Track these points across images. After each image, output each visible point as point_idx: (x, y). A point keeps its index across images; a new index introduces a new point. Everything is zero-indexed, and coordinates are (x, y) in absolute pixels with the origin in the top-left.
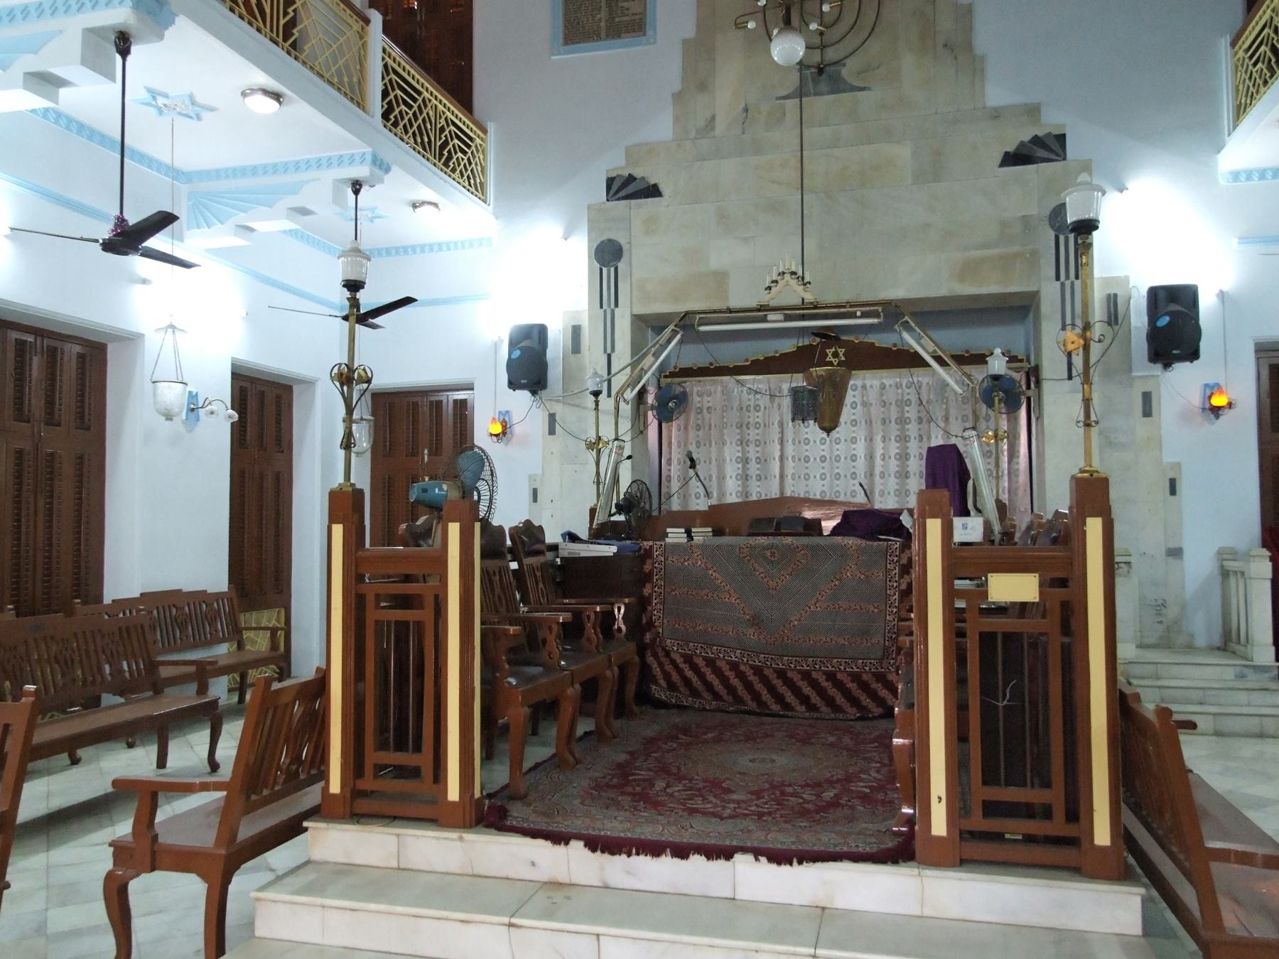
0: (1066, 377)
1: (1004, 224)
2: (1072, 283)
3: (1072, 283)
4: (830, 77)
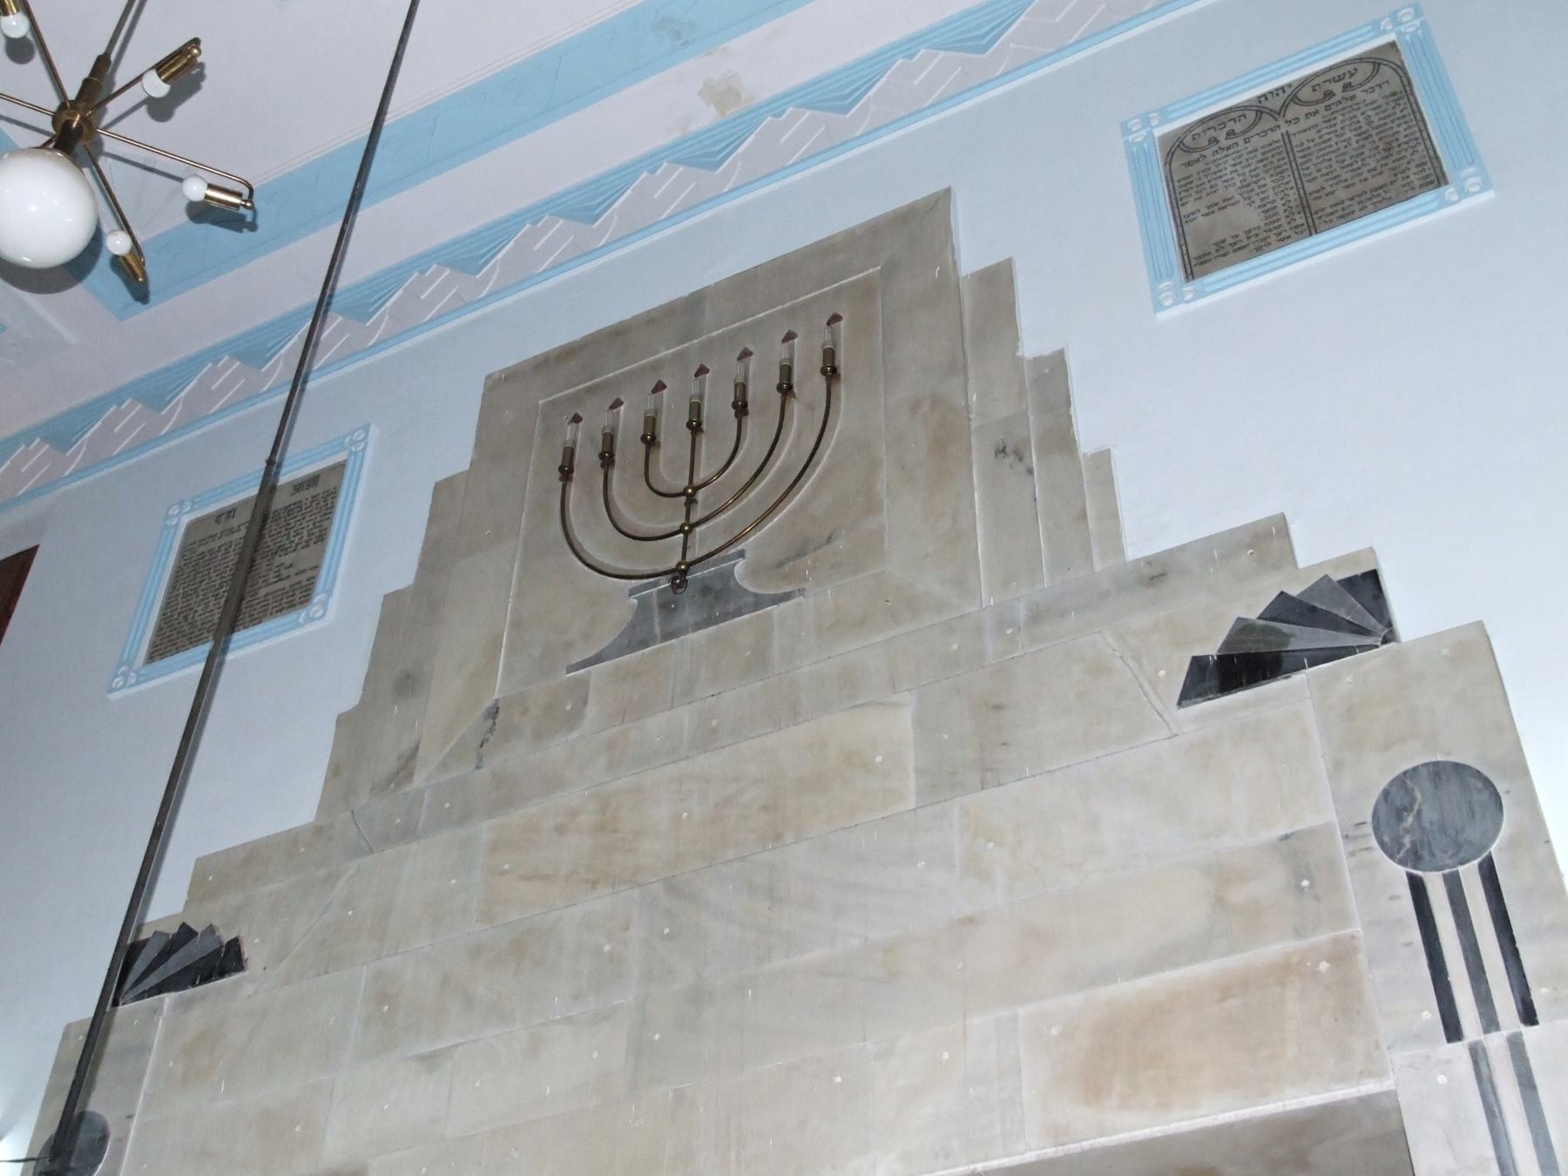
1: (1222, 876)
2: (1516, 1046)
3: (1516, 1046)
4: (706, 590)
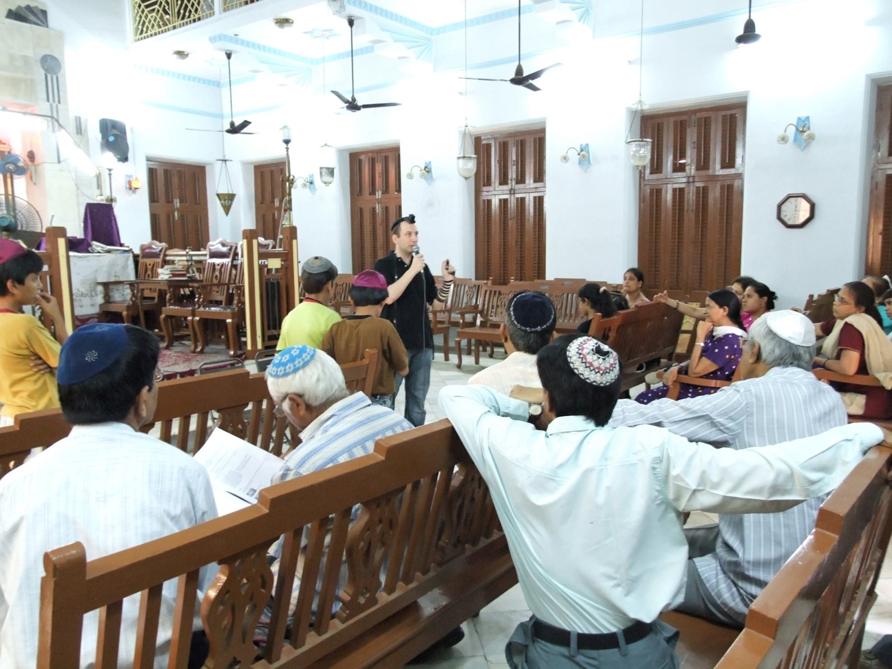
0: (56, 161)
2: (57, 106)
3: (57, 106)
